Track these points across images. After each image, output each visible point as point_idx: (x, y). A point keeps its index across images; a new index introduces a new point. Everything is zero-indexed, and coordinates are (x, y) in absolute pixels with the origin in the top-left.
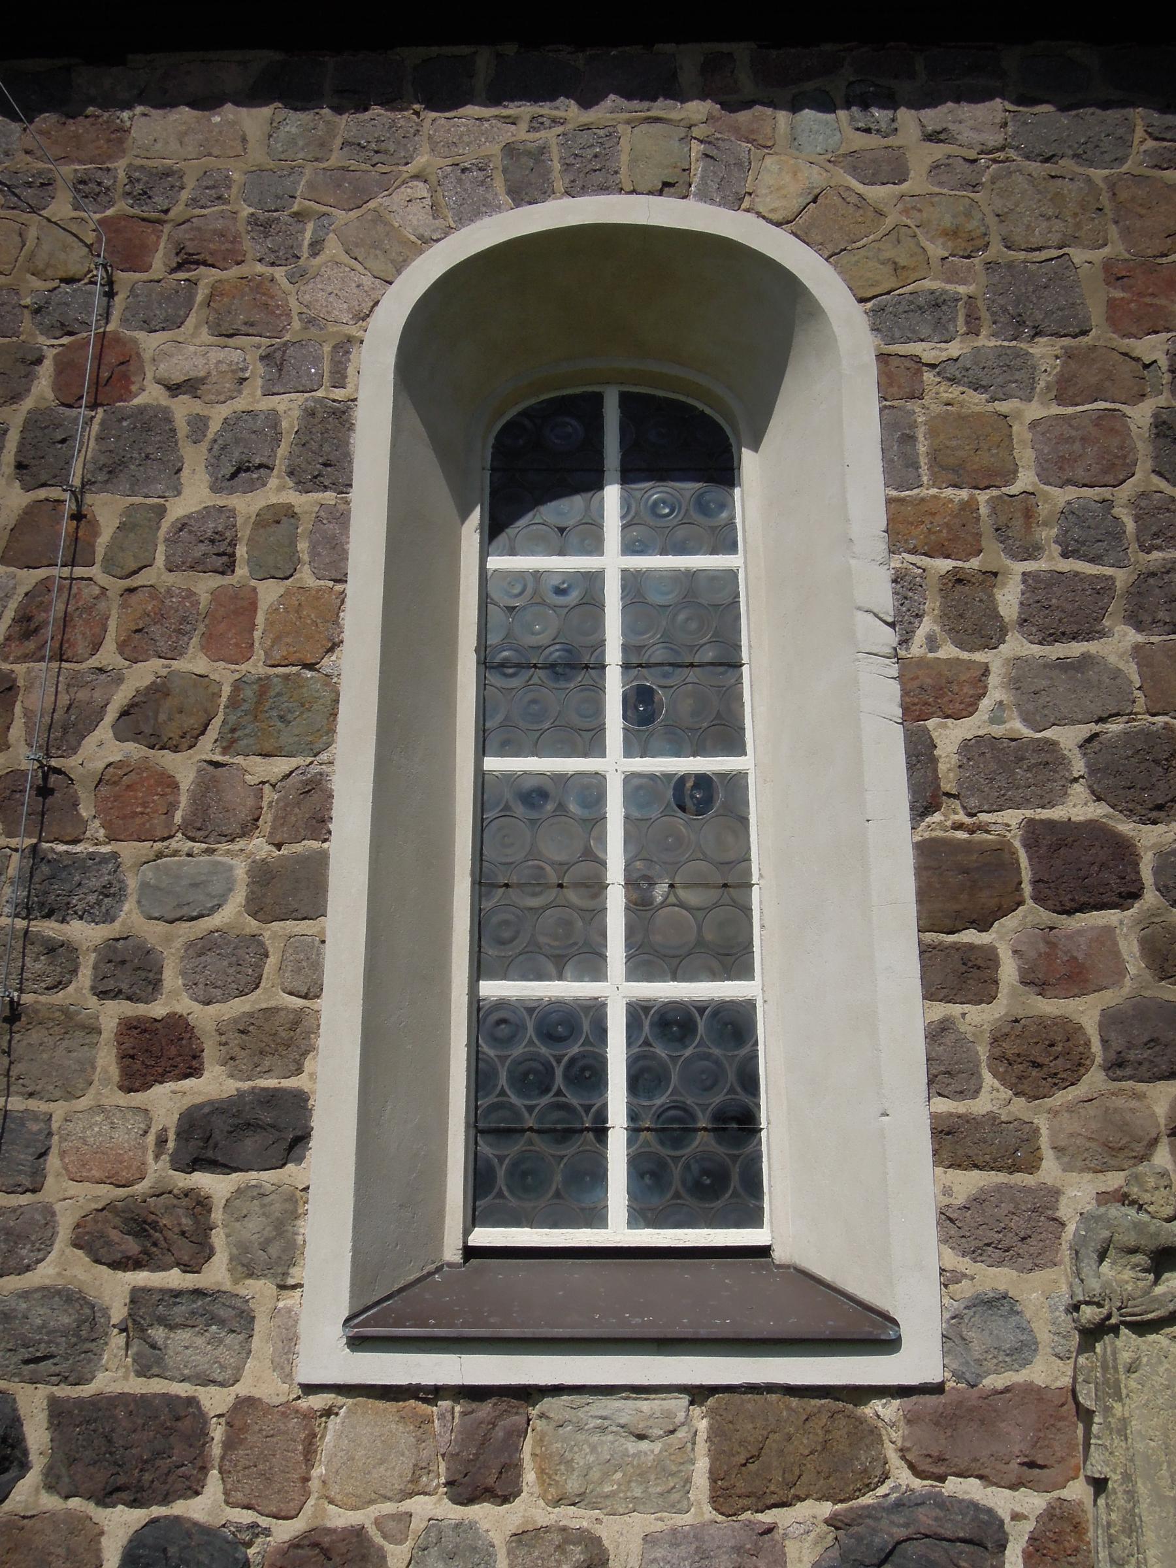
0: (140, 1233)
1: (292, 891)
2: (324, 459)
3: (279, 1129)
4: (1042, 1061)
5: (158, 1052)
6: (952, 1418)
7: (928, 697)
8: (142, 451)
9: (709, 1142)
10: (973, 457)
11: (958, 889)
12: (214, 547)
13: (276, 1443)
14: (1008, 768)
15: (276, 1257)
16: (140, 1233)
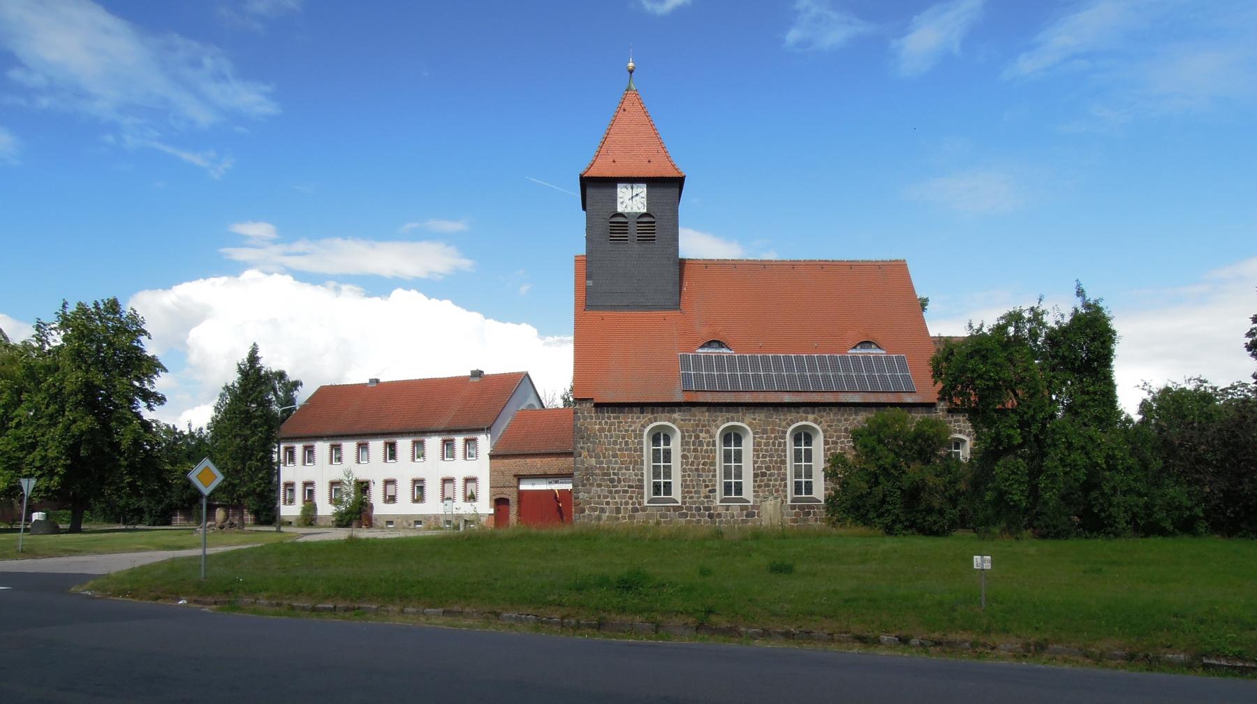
0: (706, 497)
1: (714, 476)
2: (714, 445)
3: (714, 491)
4: (760, 486)
5: (707, 486)
6: (753, 507)
7: (755, 462)
8: (701, 444)
9: (739, 490)
10: (759, 444)
11: (756, 476)
12: (706, 451)
13: (715, 508)
14: (760, 468)
16: (706, 497)
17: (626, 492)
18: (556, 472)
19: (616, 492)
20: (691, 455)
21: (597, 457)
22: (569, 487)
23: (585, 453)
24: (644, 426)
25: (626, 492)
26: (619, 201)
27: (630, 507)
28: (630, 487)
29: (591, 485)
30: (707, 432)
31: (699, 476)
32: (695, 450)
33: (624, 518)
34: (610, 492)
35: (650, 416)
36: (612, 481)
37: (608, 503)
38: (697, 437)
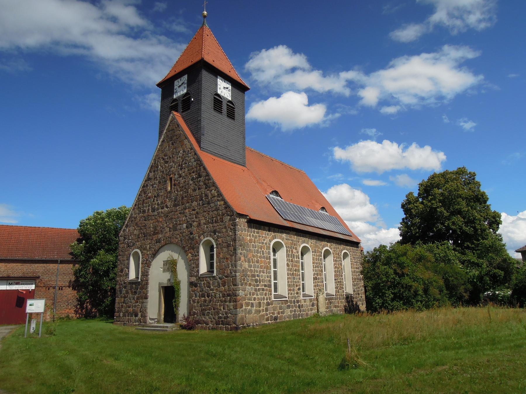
0: (297, 293)
5: (297, 286)
8: (294, 257)
15: (300, 294)
16: (297, 293)
17: (263, 290)
18: (20, 275)
19: (259, 290)
20: (290, 263)
21: (249, 262)
22: (33, 287)
23: (243, 258)
24: (270, 241)
25: (263, 290)
26: (219, 87)
27: (265, 301)
28: (265, 286)
29: (246, 284)
30: (296, 249)
31: (294, 278)
32: (292, 261)
33: (263, 310)
34: (256, 290)
35: (273, 234)
36: (256, 281)
37: (255, 299)
38: (292, 252)
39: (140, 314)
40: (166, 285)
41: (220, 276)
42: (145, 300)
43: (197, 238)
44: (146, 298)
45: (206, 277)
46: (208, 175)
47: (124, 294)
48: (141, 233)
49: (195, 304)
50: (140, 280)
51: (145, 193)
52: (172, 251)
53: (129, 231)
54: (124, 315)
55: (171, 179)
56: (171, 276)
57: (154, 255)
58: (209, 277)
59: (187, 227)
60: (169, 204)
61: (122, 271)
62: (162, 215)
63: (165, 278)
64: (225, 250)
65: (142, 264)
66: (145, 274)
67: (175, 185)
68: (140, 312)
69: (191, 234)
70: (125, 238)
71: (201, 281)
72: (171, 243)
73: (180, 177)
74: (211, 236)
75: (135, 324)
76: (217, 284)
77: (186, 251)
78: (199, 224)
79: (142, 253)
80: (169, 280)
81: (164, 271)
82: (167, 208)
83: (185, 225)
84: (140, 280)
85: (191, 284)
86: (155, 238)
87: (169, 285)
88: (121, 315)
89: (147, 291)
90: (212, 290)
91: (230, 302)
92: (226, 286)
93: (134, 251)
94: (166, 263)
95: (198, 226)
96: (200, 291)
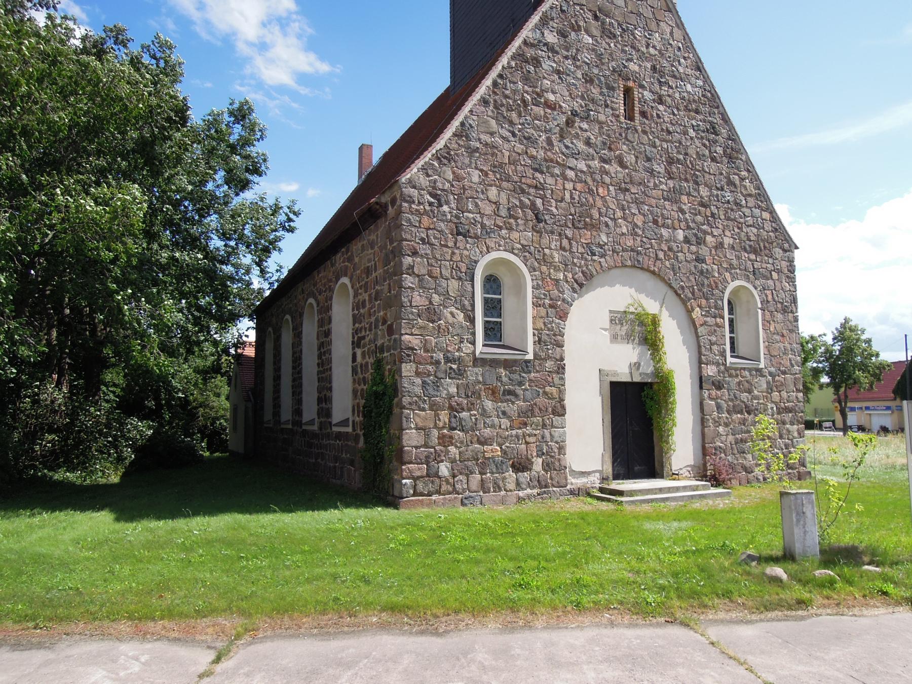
39: (538, 464)
40: (626, 378)
41: (773, 369)
42: (557, 420)
43: (717, 275)
44: (560, 410)
45: (744, 369)
46: (733, 137)
47: (450, 397)
48: (522, 206)
49: (721, 429)
50: (530, 356)
51: (526, 79)
52: (639, 290)
53: (458, 178)
54: (461, 468)
55: (628, 92)
56: (641, 355)
57: (581, 286)
58: (750, 370)
59: (687, 240)
60: (630, 159)
61: (432, 314)
62: (607, 180)
63: (625, 361)
64: (779, 316)
65: (536, 305)
66: (551, 340)
67: (643, 114)
68: (541, 454)
69: (700, 260)
70: (438, 199)
71: (730, 376)
72: (638, 266)
73: (661, 101)
74: (747, 279)
75: (521, 494)
76: (765, 386)
77: (684, 302)
78: (720, 246)
79: (532, 269)
80: (637, 365)
81: (614, 338)
82: (622, 165)
83: (680, 235)
84: (530, 356)
85: (701, 382)
86: (587, 236)
87: (637, 379)
88: (444, 469)
89: (561, 392)
90: (757, 398)
91: (792, 424)
92: (784, 394)
93: (494, 255)
94: (618, 319)
95: (716, 248)
96: (732, 400)
